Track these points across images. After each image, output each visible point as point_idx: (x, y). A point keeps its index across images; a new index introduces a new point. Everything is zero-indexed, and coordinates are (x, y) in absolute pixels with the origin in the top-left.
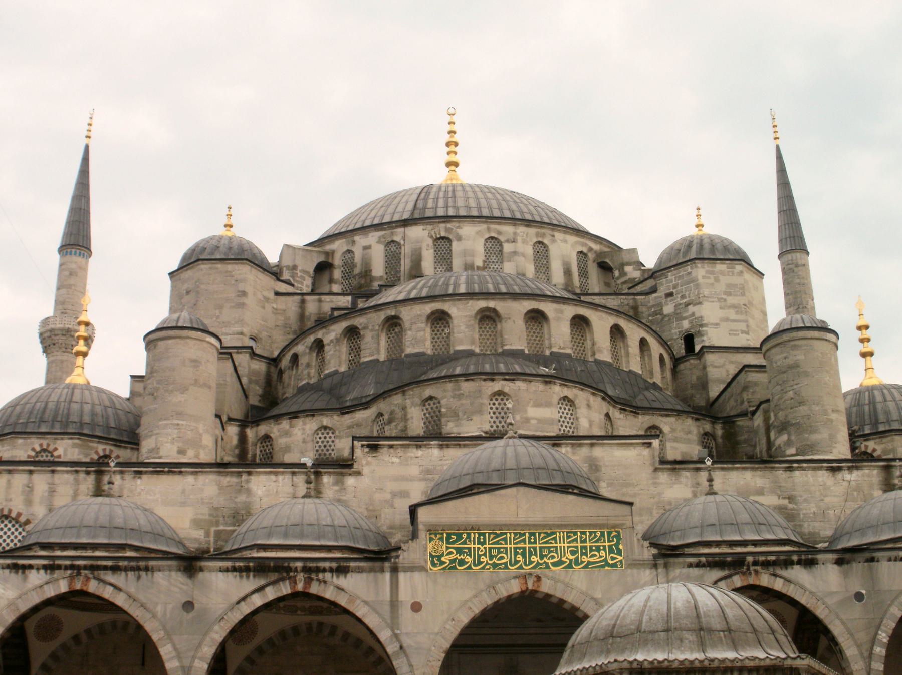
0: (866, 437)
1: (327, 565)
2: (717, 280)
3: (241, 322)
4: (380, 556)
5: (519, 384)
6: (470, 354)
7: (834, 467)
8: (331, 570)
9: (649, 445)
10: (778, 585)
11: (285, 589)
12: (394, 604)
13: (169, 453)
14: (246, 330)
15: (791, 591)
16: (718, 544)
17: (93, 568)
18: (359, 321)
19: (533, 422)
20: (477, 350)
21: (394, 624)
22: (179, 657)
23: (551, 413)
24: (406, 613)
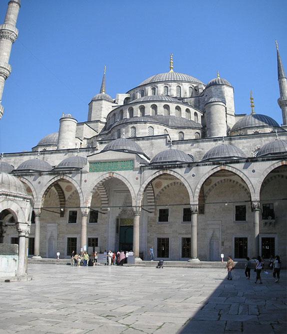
0: (240, 130)
1: (67, 172)
2: (217, 90)
3: (101, 114)
4: (78, 170)
5: (138, 124)
6: (137, 117)
7: (216, 140)
8: (68, 173)
9: (166, 137)
10: (172, 173)
11: (59, 178)
12: (81, 180)
13: (61, 148)
14: (102, 116)
15: (175, 175)
16: (159, 163)
17: (22, 175)
18: (115, 111)
19: (141, 133)
20: (139, 116)
21: (80, 185)
22: (36, 195)
23: (147, 131)
24: (83, 182)
